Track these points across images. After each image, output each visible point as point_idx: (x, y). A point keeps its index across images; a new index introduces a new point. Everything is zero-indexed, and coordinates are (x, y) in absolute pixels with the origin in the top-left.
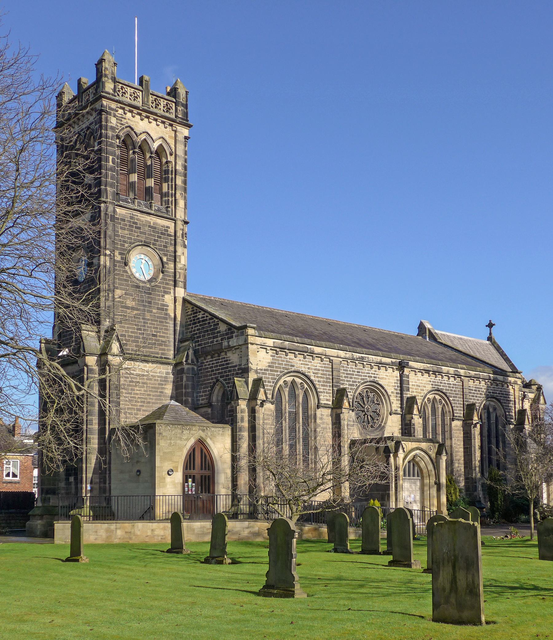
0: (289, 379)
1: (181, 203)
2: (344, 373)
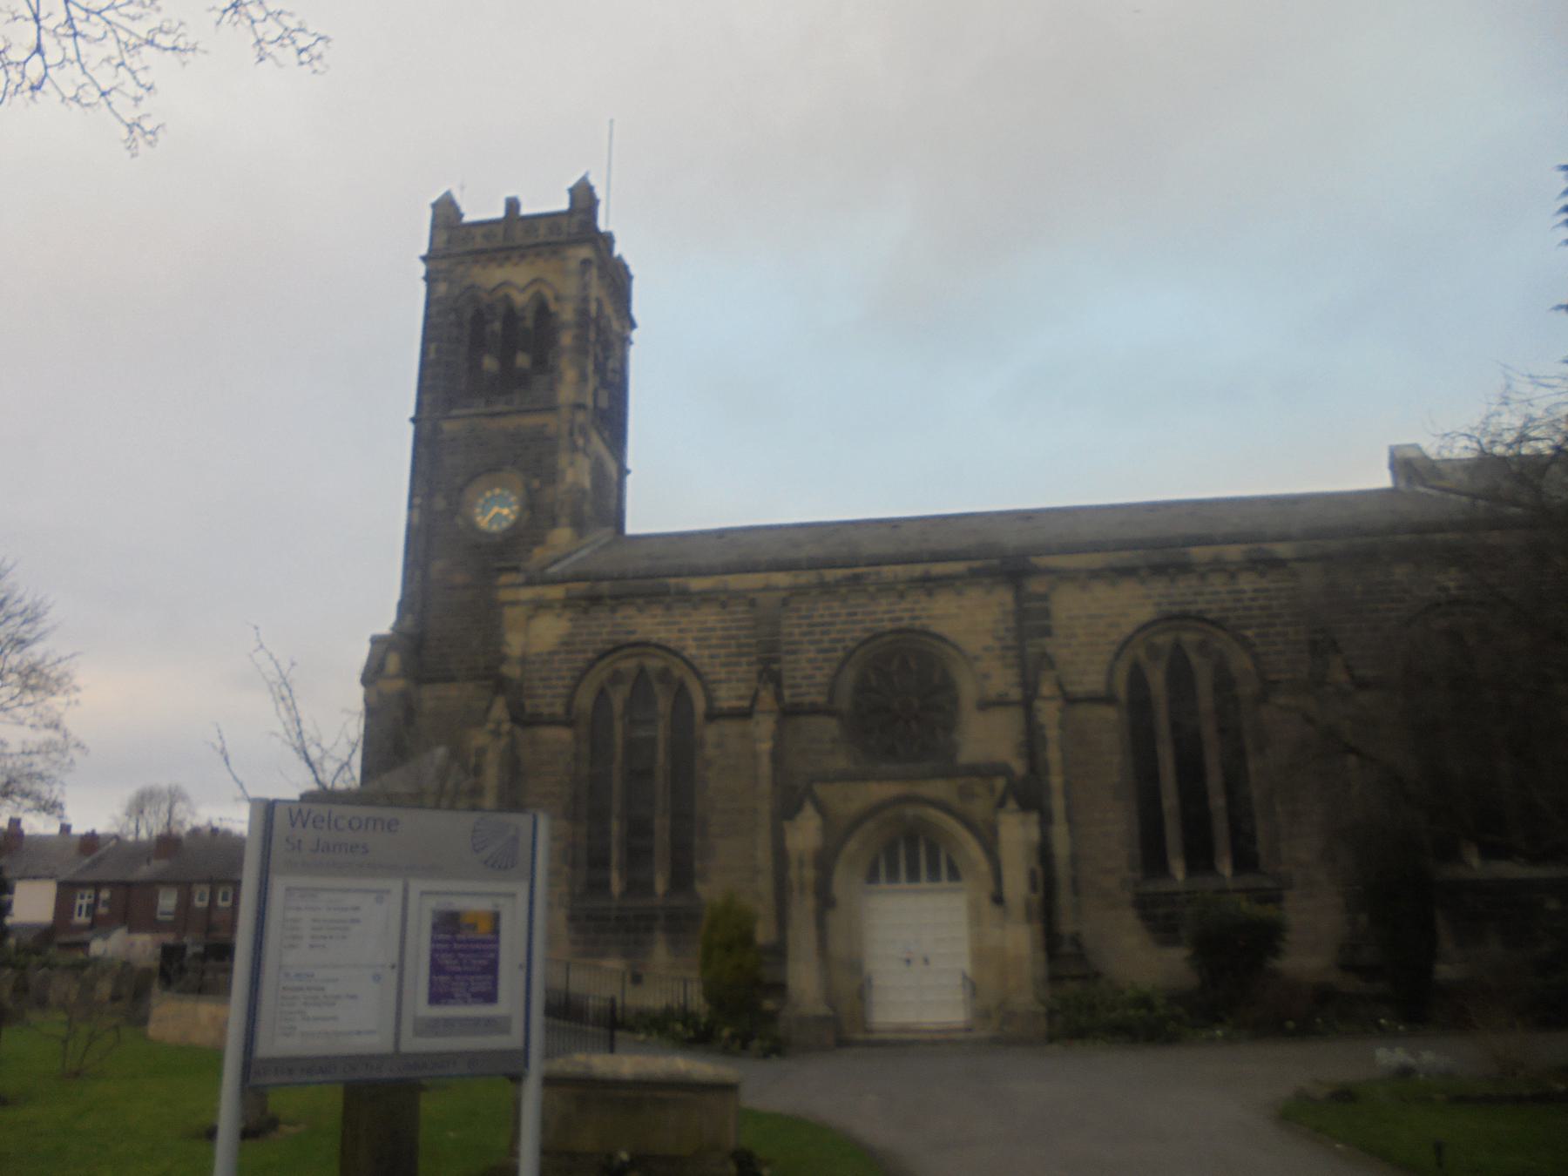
0: (628, 665)
2: (799, 626)
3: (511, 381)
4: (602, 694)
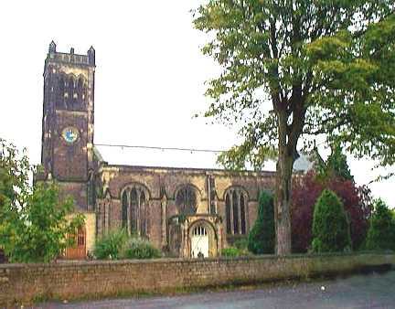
0: (131, 187)
1: (91, 104)
3: (72, 101)
4: (125, 193)
